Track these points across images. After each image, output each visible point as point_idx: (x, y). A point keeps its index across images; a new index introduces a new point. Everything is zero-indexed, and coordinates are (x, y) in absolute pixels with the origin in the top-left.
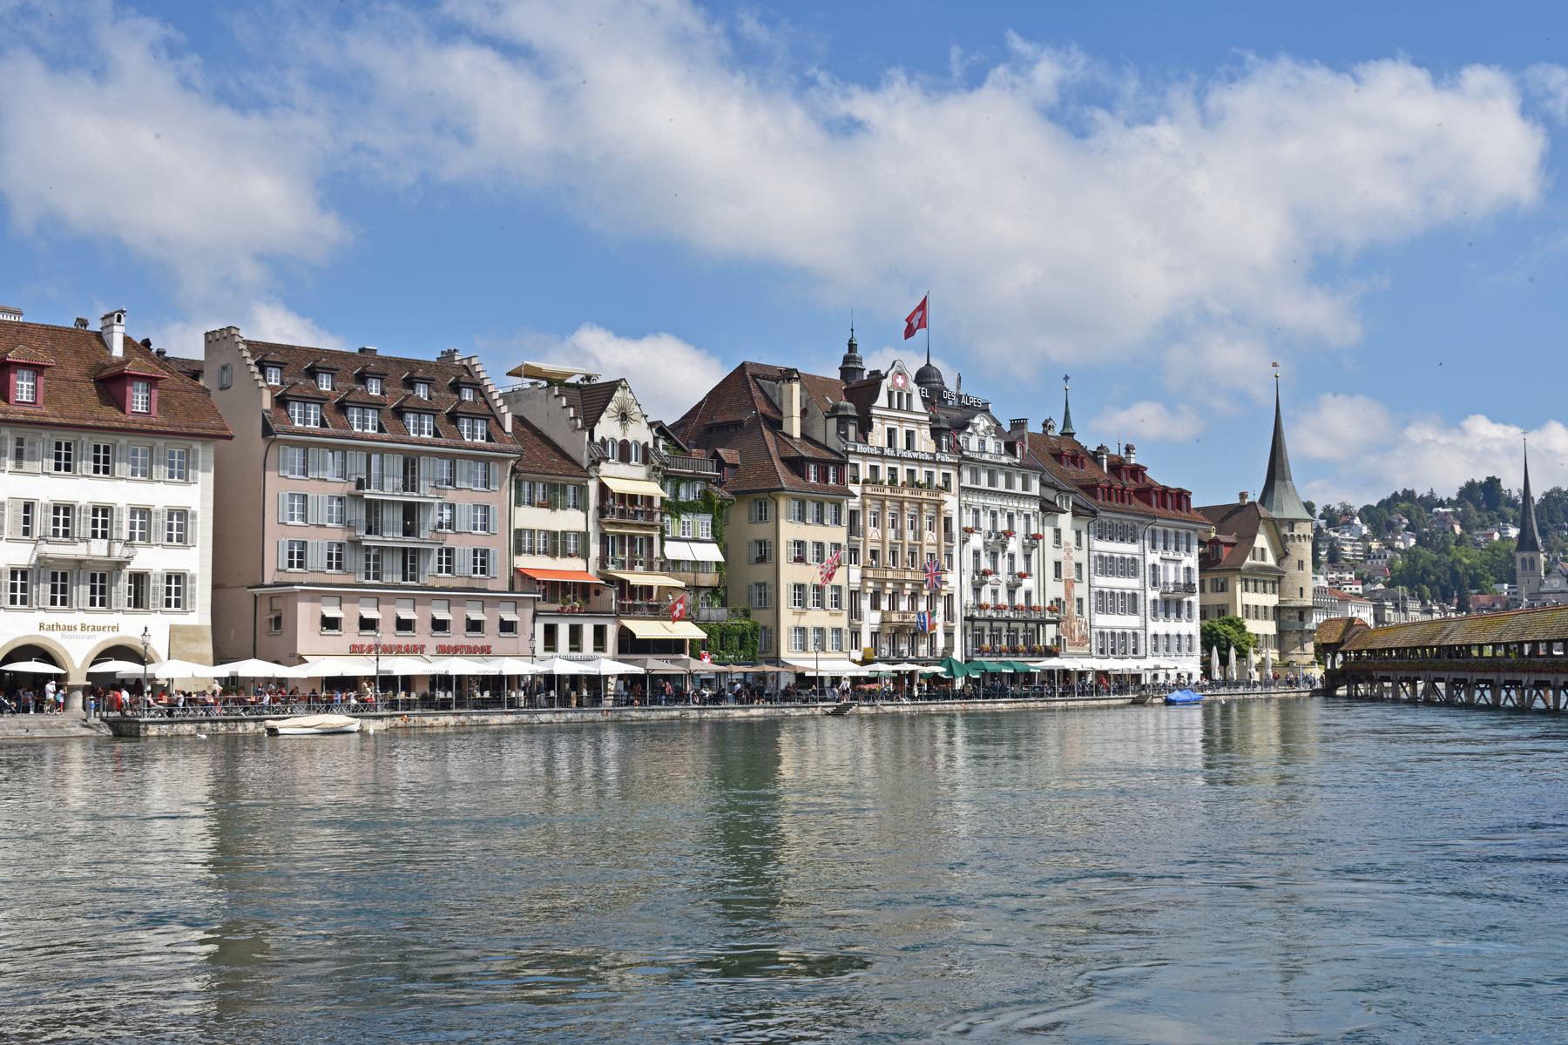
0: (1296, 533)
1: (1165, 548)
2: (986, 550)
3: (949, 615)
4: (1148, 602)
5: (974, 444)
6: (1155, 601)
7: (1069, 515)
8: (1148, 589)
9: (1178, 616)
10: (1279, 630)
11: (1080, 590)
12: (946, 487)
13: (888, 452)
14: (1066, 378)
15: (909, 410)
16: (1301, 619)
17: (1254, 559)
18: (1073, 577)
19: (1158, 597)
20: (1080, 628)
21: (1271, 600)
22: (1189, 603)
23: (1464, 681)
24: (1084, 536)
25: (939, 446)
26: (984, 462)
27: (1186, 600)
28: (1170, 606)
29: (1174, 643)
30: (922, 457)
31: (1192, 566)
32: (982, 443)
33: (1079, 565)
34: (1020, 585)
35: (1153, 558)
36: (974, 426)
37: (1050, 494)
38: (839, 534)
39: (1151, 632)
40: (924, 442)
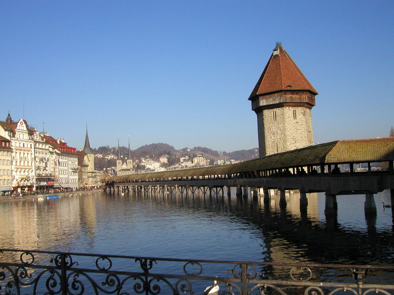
8: (69, 169)
13: (19, 139)
14: (44, 123)
25: (30, 139)
30: (26, 140)
38: (9, 158)
40: (26, 136)
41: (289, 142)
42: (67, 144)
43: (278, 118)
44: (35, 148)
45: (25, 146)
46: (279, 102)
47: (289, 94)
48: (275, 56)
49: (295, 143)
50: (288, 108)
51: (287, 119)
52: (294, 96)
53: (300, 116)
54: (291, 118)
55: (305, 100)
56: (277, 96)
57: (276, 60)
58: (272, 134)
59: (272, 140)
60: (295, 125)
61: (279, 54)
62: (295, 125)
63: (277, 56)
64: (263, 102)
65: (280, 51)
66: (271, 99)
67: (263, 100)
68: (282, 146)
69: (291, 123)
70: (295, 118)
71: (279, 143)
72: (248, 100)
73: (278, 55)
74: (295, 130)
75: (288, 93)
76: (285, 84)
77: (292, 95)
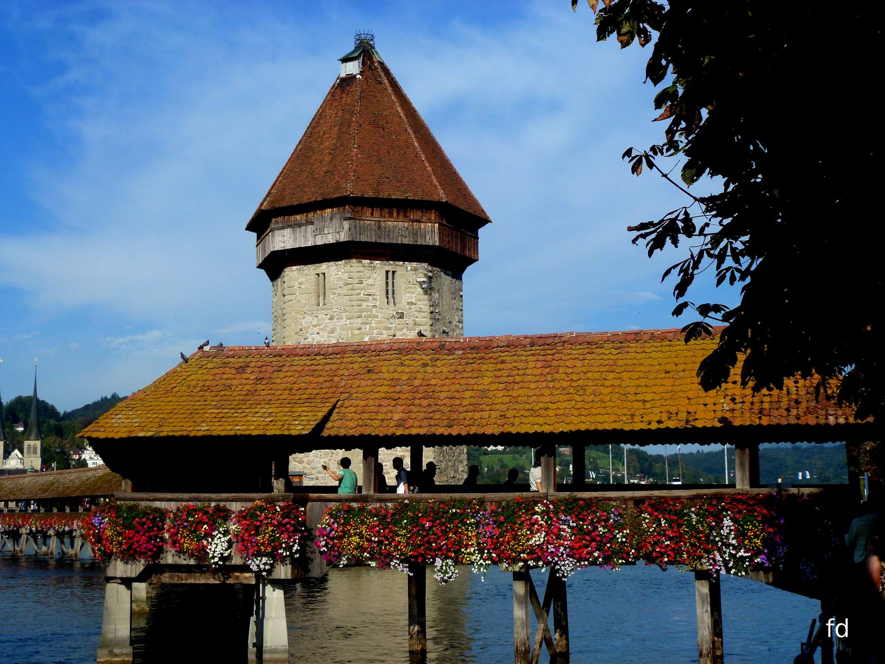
43: (330, 296)
47: (372, 214)
48: (343, 80)
50: (369, 261)
54: (375, 300)
55: (428, 238)
56: (331, 219)
57: (344, 95)
60: (391, 323)
62: (390, 325)
63: (350, 78)
64: (284, 236)
65: (364, 64)
66: (310, 228)
67: (283, 228)
69: (377, 317)
72: (247, 229)
73: (354, 77)
75: (370, 211)
76: (358, 178)
77: (384, 217)
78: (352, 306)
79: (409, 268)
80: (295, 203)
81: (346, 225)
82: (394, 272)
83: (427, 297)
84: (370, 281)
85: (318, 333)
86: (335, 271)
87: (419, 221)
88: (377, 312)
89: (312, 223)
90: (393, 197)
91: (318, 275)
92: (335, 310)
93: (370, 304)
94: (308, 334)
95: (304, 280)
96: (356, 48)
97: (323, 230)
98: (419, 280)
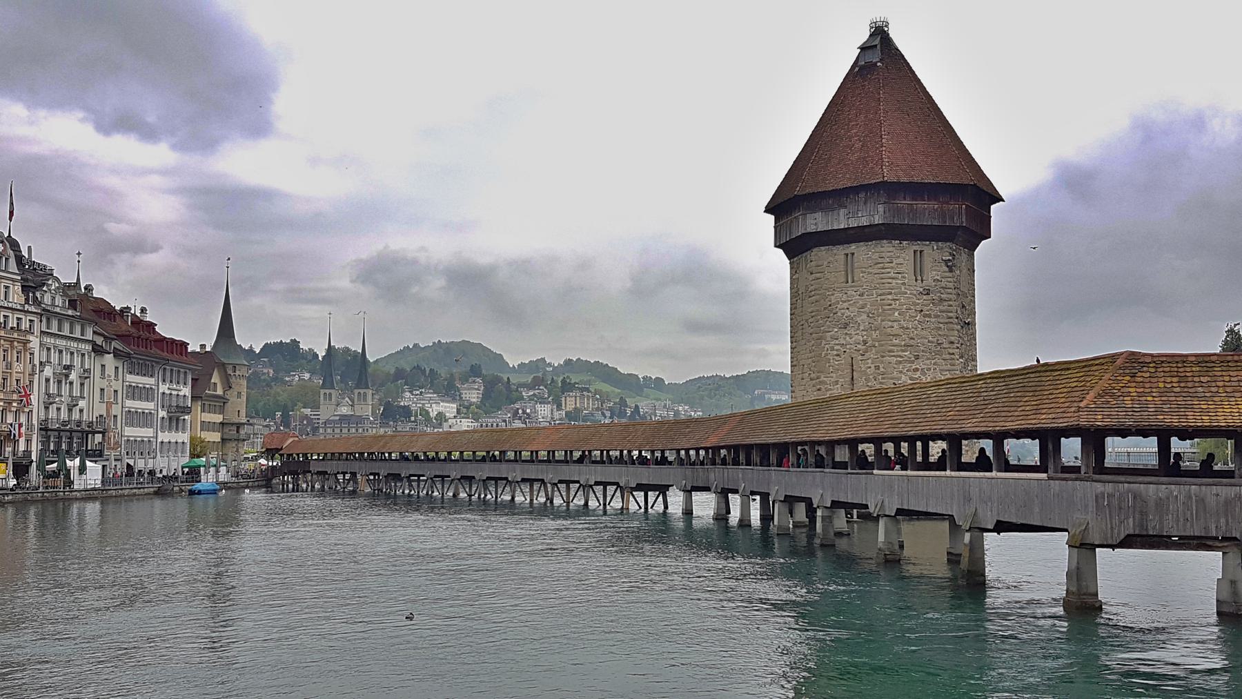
0: (237, 373)
1: (171, 382)
2: (54, 378)
3: (30, 427)
4: (159, 419)
5: (47, 299)
6: (163, 418)
7: (112, 355)
8: (160, 410)
9: (177, 429)
10: (223, 439)
11: (116, 410)
12: (30, 331)
14: (79, 254)
15: (6, 271)
16: (238, 432)
17: (209, 390)
18: (112, 400)
19: (166, 416)
20: (115, 437)
21: (218, 418)
22: (184, 419)
23: (542, 481)
24: (120, 370)
25: (27, 301)
26: (56, 313)
27: (182, 418)
28: (175, 419)
29: (173, 448)
31: (187, 394)
32: (53, 299)
33: (116, 391)
34: (78, 405)
35: (164, 388)
36: (48, 285)
37: (99, 340)
39: (159, 440)
40: (16, 296)
41: (893, 354)
42: (156, 325)
43: (858, 274)
44: (41, 332)
45: (12, 323)
46: (868, 224)
48: (862, 68)
49: (913, 359)
51: (890, 281)
52: (921, 205)
53: (934, 273)
54: (904, 277)
55: (955, 219)
58: (835, 325)
59: (838, 347)
60: (919, 299)
61: (878, 60)
62: (919, 301)
66: (842, 211)
68: (870, 367)
69: (906, 293)
70: (919, 278)
71: (860, 358)
74: (917, 316)
75: (903, 195)
78: (883, 284)
79: (935, 248)
80: (831, 189)
81: (881, 208)
82: (921, 252)
83: (950, 274)
84: (900, 260)
85: (848, 309)
86: (863, 252)
87: (947, 203)
88: (905, 289)
89: (846, 207)
90: (926, 181)
91: (845, 254)
92: (864, 287)
93: (899, 282)
94: (837, 310)
95: (832, 259)
96: (871, 35)
97: (857, 214)
98: (944, 258)
